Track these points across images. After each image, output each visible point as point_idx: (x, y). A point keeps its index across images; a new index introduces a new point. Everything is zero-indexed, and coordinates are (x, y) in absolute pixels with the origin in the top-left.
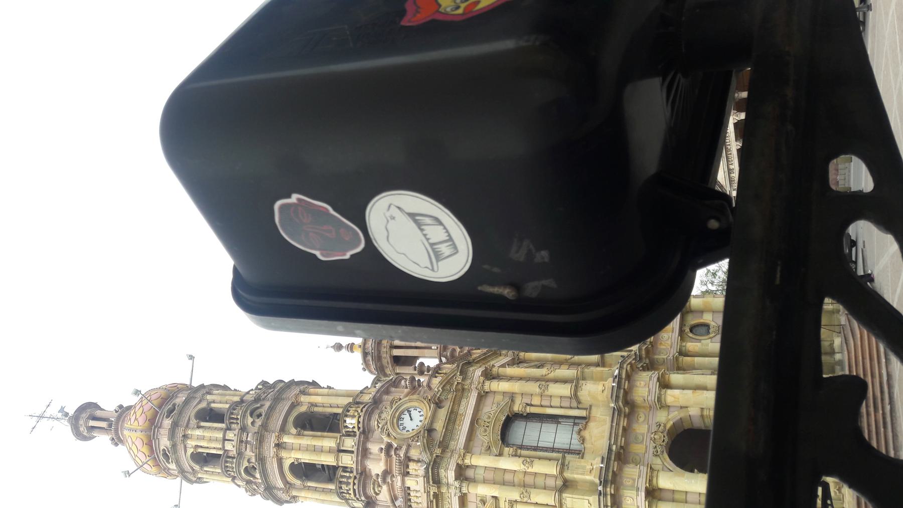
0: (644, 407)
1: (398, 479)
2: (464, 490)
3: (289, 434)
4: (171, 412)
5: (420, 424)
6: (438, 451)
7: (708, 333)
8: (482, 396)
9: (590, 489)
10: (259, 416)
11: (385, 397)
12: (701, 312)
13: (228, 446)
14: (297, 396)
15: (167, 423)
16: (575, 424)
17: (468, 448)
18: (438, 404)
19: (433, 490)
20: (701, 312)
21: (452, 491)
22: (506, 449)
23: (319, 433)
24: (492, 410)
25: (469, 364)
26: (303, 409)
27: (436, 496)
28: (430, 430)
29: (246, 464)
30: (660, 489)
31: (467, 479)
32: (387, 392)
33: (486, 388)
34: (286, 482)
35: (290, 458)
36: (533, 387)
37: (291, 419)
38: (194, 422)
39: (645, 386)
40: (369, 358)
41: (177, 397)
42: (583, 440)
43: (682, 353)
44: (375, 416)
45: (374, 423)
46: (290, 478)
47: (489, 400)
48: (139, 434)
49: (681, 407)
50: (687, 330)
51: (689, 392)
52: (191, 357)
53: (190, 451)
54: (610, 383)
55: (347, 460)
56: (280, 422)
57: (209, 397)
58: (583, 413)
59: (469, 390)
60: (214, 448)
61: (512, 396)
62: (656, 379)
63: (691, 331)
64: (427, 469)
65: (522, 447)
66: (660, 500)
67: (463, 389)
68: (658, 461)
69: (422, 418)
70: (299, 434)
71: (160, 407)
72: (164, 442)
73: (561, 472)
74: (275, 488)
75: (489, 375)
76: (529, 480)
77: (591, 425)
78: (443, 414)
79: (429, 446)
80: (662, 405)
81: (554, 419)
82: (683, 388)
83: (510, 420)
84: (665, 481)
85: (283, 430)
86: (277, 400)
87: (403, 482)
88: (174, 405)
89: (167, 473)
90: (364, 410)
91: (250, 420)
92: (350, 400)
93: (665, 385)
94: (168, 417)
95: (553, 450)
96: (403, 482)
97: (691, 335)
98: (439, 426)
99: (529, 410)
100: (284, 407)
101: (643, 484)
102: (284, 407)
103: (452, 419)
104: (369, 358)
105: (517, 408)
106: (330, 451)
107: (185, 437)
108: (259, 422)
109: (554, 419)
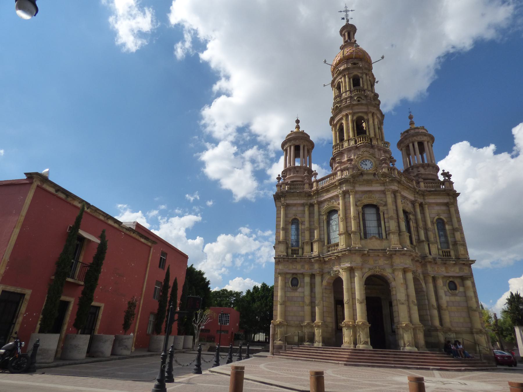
0: (392, 262)
1: (339, 168)
2: (340, 195)
3: (353, 117)
4: (354, 64)
5: (365, 169)
6: (352, 181)
7: (451, 290)
8: (384, 192)
9: (348, 245)
10: (359, 101)
11: (376, 150)
12: (463, 285)
14: (370, 112)
15: (350, 65)
16: (379, 234)
17: (356, 192)
18: (374, 174)
19: (337, 183)
20: (463, 285)
21: (339, 190)
22: (361, 208)
23: (355, 129)
25: (399, 182)
26: (366, 117)
27: (336, 185)
28: (362, 174)
29: (338, 106)
30: (354, 273)
31: (344, 195)
32: (379, 150)
33: (387, 193)
34: (336, 124)
35: (344, 122)
36: (392, 213)
37: (360, 115)
38: (352, 75)
39: (400, 262)
40: (406, 134)
42: (371, 239)
43: (434, 279)
44: (365, 149)
45: (362, 150)
47: (382, 196)
48: (342, 56)
49: (394, 279)
50: (451, 279)
51: (402, 281)
52: (383, 58)
53: (340, 80)
54: (398, 247)
55: (346, 145)
56: (357, 111)
57: (364, 75)
58: (384, 236)
59: (384, 186)
60: (342, 90)
61: (386, 205)
62: (406, 266)
63: (451, 281)
64: (344, 178)
65: (363, 214)
66: (350, 273)
67: (384, 183)
68: (367, 270)
69: (368, 169)
70: (353, 121)
71: (355, 58)
72: (342, 68)
73: (352, 232)
74: (334, 121)
75: (395, 193)
76: (348, 220)
77: (379, 242)
78: (371, 177)
79: (353, 176)
80: (394, 271)
81: (379, 225)
82: (405, 278)
83: (375, 207)
85: (353, 114)
86: (366, 105)
87: (339, 171)
88: (358, 64)
89: (333, 75)
91: (355, 98)
92: (372, 135)
93: (405, 271)
95: (365, 226)
96: (339, 171)
97: (448, 281)
98: (365, 177)
99: (381, 214)
100: (364, 109)
101: (354, 265)
102: (364, 109)
103: (369, 182)
104: (406, 134)
105: (381, 208)
106: (349, 136)
107: (344, 76)
108: (355, 103)
109: (379, 225)
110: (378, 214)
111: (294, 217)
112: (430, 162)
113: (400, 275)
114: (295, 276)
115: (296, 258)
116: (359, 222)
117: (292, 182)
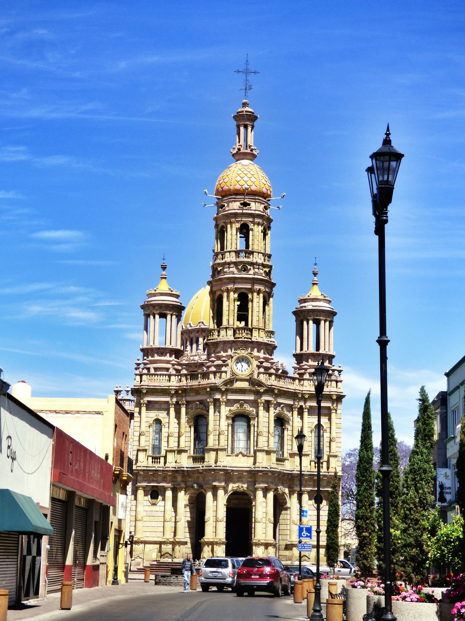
6: (223, 389)
13: (227, 254)
16: (247, 449)
24: (248, 408)
26: (250, 296)
37: (243, 291)
38: (238, 225)
41: (255, 202)
46: (218, 293)
78: (245, 385)
79: (226, 383)
84: (221, 493)
85: (235, 290)
88: (249, 205)
90: (246, 339)
94: (241, 204)
110: (249, 427)
111: (156, 418)
112: (322, 351)
113: (260, 494)
114: (155, 489)
115: (158, 470)
116: (228, 436)
117: (156, 369)
